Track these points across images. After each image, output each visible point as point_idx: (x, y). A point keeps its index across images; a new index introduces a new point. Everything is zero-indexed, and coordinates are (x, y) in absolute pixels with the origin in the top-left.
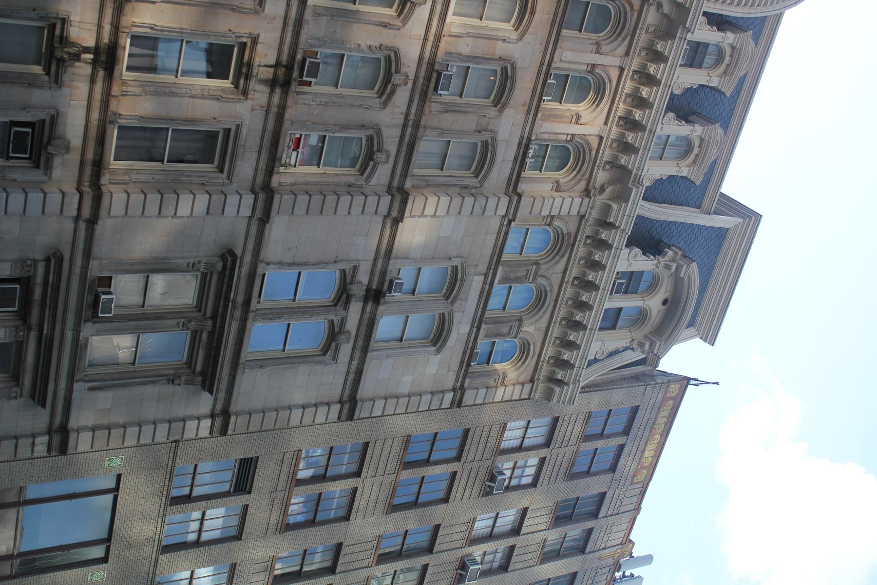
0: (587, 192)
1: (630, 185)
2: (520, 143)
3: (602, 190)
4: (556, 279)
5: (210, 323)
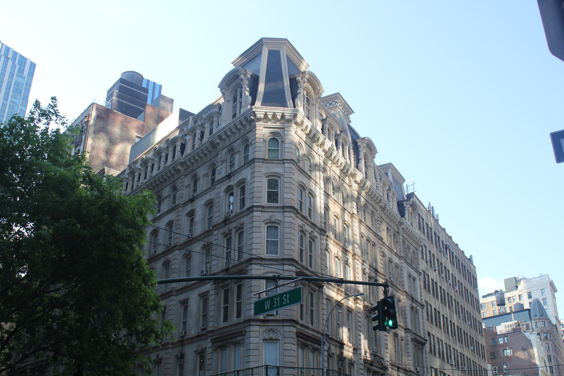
0: (398, 233)
1: (401, 221)
2: (395, 255)
3: (398, 228)
4: (407, 242)
5: (419, 344)
